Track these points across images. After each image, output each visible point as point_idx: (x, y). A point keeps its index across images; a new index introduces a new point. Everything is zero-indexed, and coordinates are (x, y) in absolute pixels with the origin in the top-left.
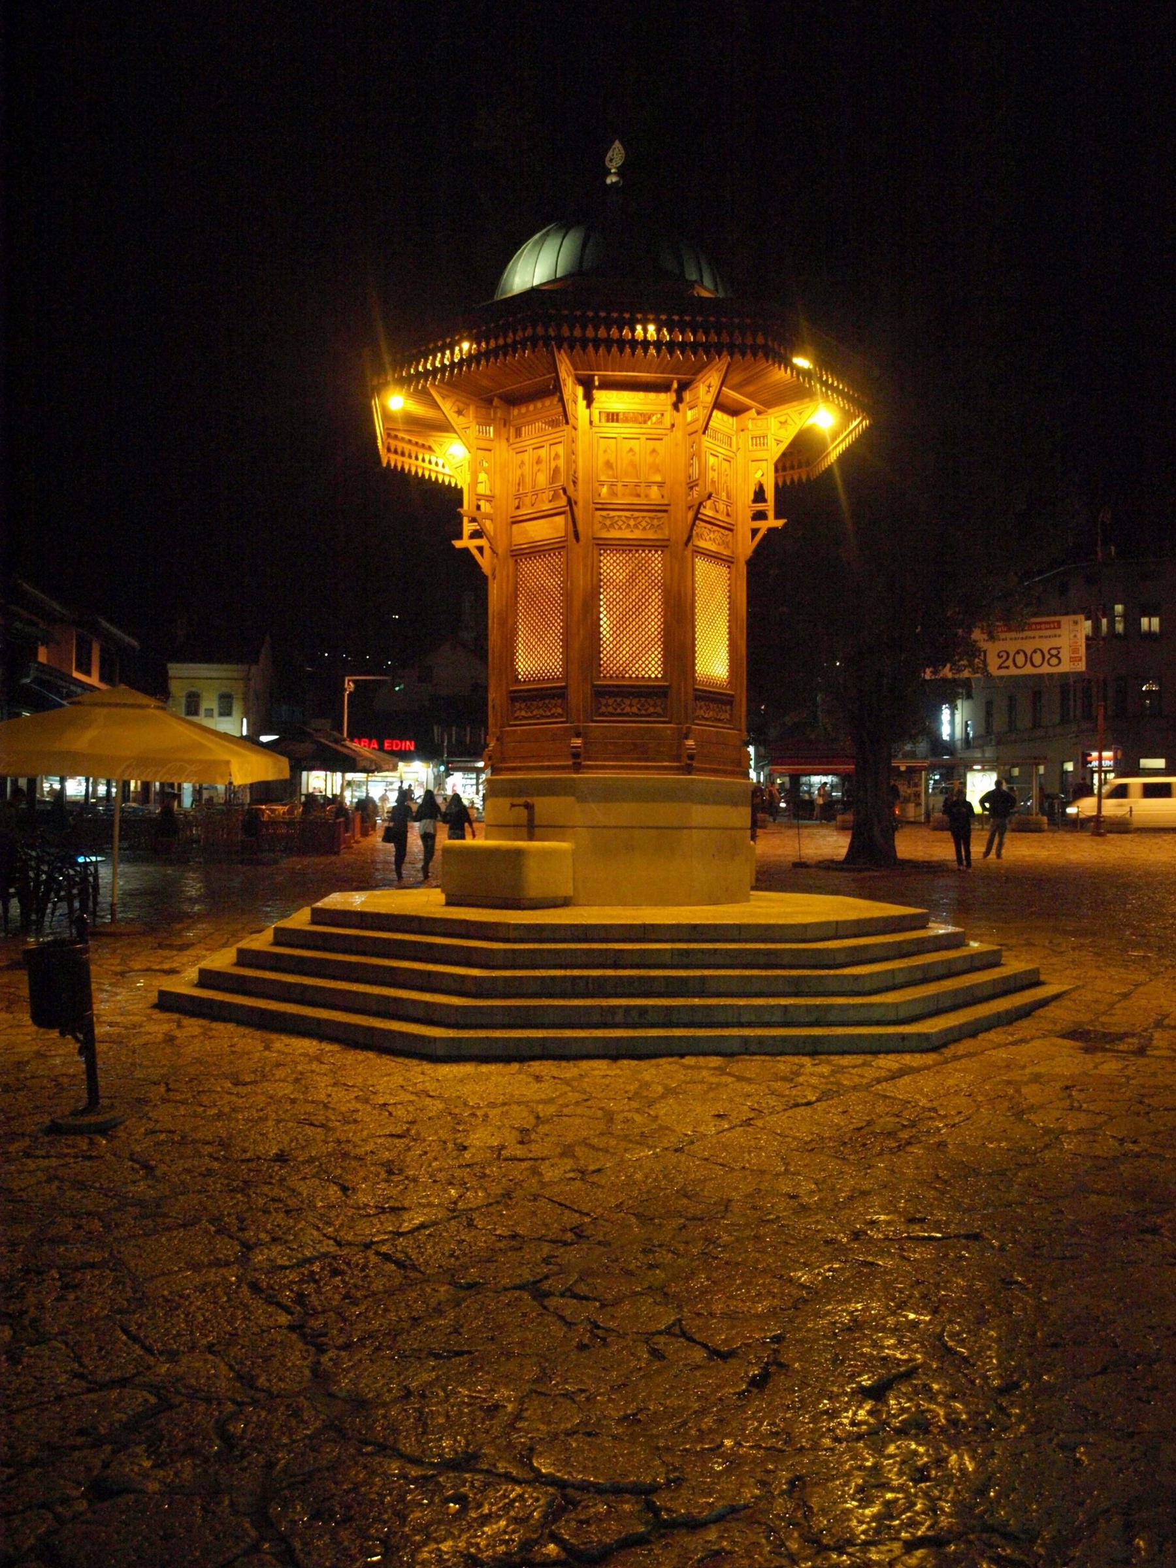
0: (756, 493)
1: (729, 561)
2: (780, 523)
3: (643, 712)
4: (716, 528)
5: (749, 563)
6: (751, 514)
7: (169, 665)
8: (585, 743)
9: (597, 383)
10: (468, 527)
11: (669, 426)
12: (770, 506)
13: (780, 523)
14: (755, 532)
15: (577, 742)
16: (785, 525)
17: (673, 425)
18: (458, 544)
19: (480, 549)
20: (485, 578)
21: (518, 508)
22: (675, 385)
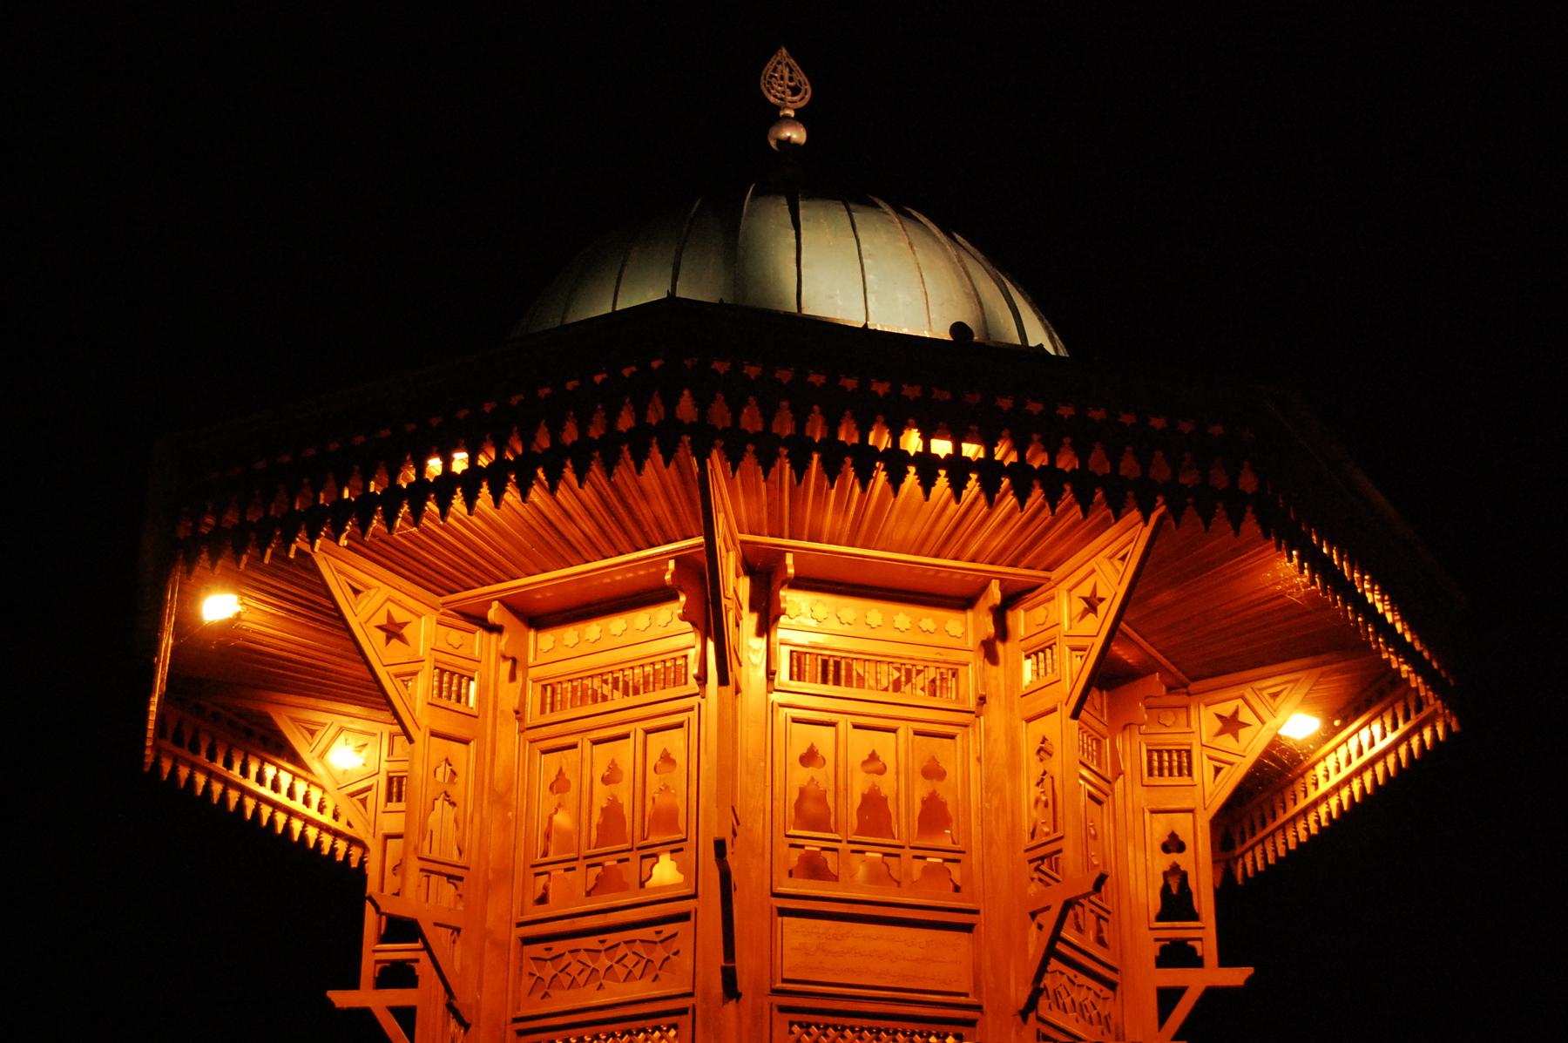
0: (1166, 890)
2: (1237, 976)
4: (1082, 979)
6: (1153, 950)
9: (791, 571)
10: (375, 953)
11: (972, 704)
12: (1204, 933)
13: (1237, 976)
14: (1168, 998)
16: (1249, 981)
17: (982, 700)
18: (341, 998)
19: (406, 1016)
21: (542, 900)
22: (995, 594)
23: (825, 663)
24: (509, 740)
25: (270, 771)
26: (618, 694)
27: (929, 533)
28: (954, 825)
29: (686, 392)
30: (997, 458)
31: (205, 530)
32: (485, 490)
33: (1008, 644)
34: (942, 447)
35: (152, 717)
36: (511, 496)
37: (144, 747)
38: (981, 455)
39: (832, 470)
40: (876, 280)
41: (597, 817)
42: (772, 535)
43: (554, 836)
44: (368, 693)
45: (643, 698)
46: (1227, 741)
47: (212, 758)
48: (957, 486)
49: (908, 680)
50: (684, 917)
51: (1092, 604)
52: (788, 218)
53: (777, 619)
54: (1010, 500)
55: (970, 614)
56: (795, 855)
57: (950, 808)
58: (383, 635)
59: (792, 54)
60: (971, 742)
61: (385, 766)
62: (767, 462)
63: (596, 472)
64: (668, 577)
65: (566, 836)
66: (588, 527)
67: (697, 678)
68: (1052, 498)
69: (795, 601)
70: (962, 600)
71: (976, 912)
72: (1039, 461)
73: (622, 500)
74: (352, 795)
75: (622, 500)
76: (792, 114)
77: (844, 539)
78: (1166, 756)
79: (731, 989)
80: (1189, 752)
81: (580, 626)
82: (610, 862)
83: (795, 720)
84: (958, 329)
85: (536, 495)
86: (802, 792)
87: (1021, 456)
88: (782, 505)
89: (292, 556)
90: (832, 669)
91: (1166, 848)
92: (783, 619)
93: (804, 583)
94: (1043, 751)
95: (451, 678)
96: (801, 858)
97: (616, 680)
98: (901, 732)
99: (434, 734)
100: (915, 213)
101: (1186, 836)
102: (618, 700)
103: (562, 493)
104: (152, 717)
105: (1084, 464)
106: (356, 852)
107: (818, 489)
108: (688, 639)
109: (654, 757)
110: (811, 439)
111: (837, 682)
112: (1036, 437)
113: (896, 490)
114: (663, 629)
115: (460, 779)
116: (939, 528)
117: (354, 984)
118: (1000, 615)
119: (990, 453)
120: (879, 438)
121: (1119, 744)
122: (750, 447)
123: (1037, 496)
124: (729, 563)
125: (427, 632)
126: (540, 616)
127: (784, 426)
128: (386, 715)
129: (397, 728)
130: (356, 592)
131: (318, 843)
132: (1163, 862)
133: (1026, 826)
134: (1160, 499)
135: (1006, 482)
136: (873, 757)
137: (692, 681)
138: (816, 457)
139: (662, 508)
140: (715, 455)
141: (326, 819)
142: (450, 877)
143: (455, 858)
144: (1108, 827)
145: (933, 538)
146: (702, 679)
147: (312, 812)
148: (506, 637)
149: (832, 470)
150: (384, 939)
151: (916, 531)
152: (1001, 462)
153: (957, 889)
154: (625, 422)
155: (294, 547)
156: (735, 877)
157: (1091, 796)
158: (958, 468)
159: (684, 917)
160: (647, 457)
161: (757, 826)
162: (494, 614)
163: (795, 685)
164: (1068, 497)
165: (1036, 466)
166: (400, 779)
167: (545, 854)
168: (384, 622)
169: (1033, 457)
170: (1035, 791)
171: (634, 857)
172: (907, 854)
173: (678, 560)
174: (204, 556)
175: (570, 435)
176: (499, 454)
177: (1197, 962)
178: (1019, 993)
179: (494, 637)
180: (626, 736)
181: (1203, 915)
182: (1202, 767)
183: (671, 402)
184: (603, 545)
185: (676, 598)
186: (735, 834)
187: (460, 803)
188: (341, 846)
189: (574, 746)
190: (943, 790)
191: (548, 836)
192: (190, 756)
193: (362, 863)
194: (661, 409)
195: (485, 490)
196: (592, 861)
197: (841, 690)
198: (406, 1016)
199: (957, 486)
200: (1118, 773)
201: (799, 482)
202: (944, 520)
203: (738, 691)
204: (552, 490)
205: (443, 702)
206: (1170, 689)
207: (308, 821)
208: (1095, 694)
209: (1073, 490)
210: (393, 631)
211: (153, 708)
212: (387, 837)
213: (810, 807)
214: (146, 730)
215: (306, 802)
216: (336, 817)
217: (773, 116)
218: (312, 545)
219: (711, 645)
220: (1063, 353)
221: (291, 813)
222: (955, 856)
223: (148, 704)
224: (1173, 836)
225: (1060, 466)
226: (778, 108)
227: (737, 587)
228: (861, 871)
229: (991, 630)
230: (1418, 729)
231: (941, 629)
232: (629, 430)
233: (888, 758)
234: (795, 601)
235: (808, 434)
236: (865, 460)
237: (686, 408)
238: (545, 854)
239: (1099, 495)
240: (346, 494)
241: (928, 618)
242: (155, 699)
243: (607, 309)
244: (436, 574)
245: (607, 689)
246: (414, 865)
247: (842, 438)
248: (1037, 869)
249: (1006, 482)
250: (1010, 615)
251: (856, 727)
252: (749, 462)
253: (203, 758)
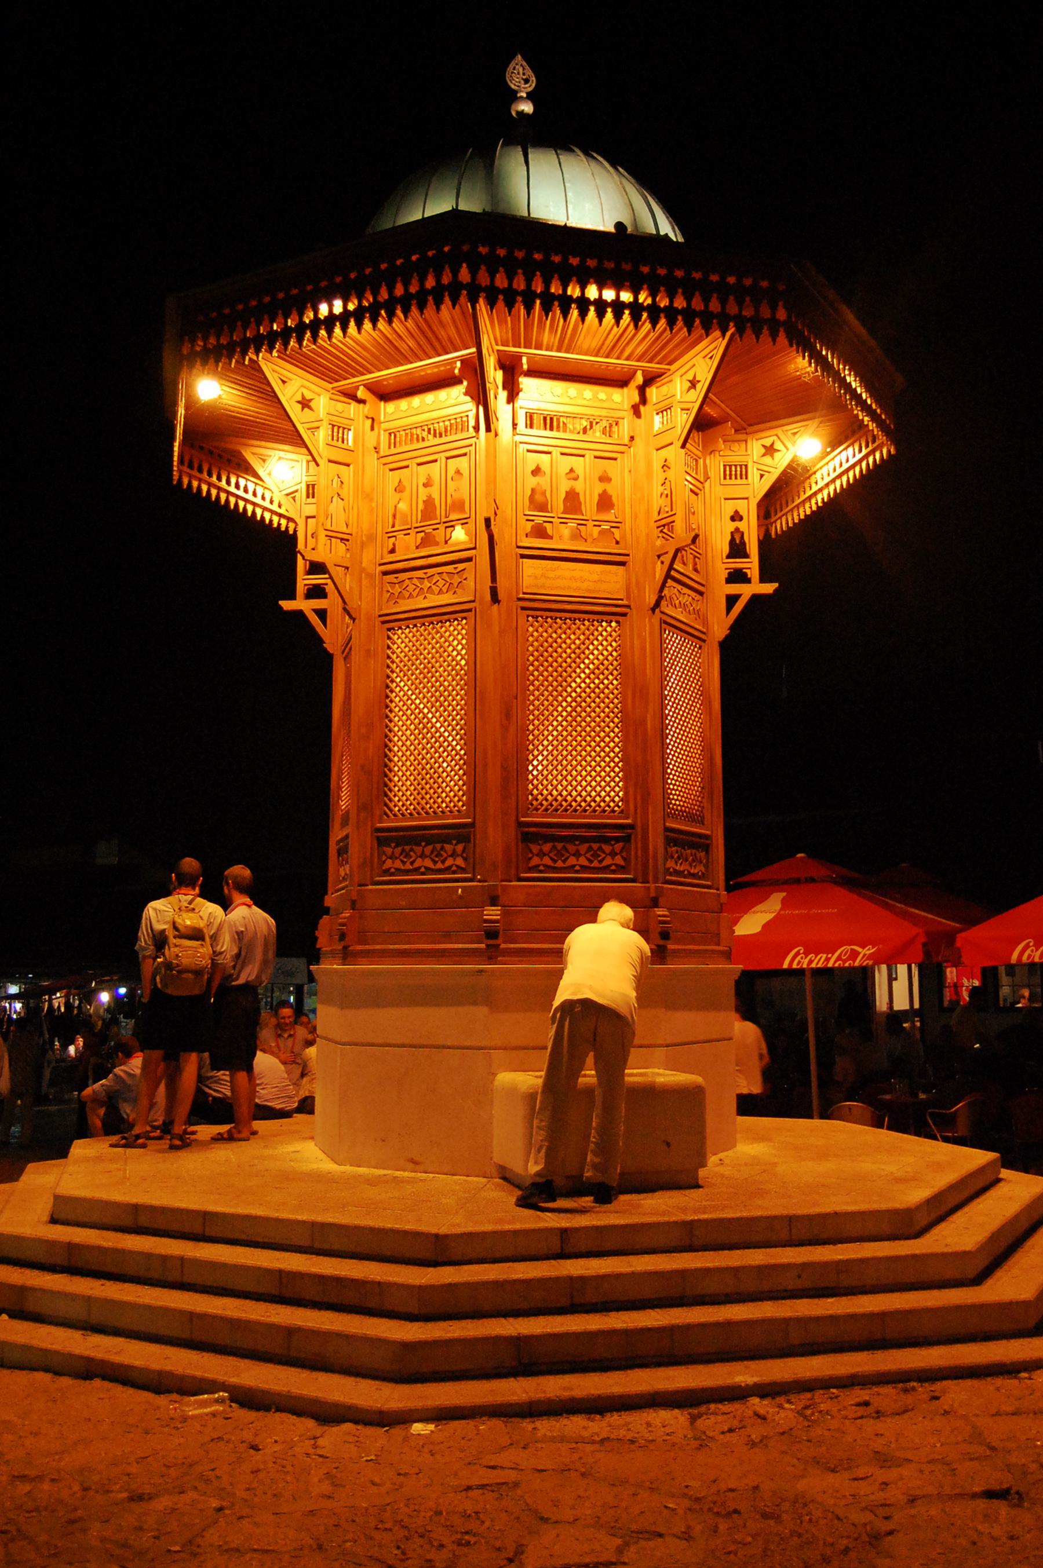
0: (732, 542)
1: (699, 638)
2: (769, 588)
3: (595, 864)
4: (685, 590)
5: (726, 646)
6: (724, 574)
8: (504, 914)
9: (525, 367)
10: (304, 580)
11: (626, 441)
12: (752, 565)
13: (769, 588)
14: (732, 600)
15: (493, 913)
16: (776, 591)
17: (632, 438)
18: (286, 605)
19: (322, 614)
20: (330, 656)
22: (639, 378)
23: (545, 419)
24: (372, 463)
25: (242, 482)
26: (430, 437)
27: (603, 344)
28: (616, 508)
29: (464, 265)
30: (641, 301)
31: (198, 349)
32: (352, 323)
33: (647, 406)
34: (609, 295)
35: (176, 454)
36: (367, 325)
37: (173, 470)
38: (631, 300)
39: (547, 309)
40: (573, 195)
41: (421, 506)
42: (514, 346)
43: (398, 516)
44: (294, 438)
45: (444, 439)
46: (767, 459)
47: (210, 475)
48: (618, 317)
49: (591, 427)
50: (469, 559)
51: (693, 384)
52: (523, 159)
53: (518, 394)
54: (648, 326)
55: (625, 390)
56: (530, 524)
57: (614, 499)
58: (300, 406)
59: (524, 58)
60: (625, 462)
61: (305, 479)
62: (510, 305)
63: (414, 311)
64: (457, 371)
65: (404, 515)
66: (411, 343)
67: (474, 428)
68: (671, 323)
69: (526, 383)
70: (621, 382)
71: (628, 555)
72: (664, 303)
73: (430, 327)
74: (287, 495)
75: (430, 327)
76: (525, 95)
77: (555, 348)
78: (733, 468)
79: (495, 598)
80: (746, 466)
81: (409, 399)
82: (429, 530)
83: (528, 451)
84: (619, 226)
85: (382, 324)
86: (533, 490)
87: (654, 300)
88: (519, 329)
89: (247, 363)
90: (550, 422)
91: (733, 519)
92: (521, 394)
93: (531, 373)
94: (665, 466)
95: (338, 429)
96: (532, 527)
97: (429, 429)
98: (587, 457)
99: (330, 461)
100: (595, 155)
101: (743, 513)
102: (432, 440)
103: (396, 324)
104: (176, 454)
105: (689, 303)
106: (292, 526)
107: (540, 320)
108: (468, 406)
109: (451, 472)
110: (535, 292)
111: (551, 429)
112: (662, 289)
113: (583, 321)
114: (454, 400)
115: (345, 486)
116: (608, 342)
117: (292, 597)
118: (642, 390)
119: (636, 299)
120: (573, 289)
121: (708, 461)
122: (501, 297)
123: (662, 323)
124: (490, 363)
125: (324, 403)
126: (386, 394)
127: (520, 284)
128: (304, 450)
129: (310, 458)
130: (284, 382)
131: (271, 521)
132: (732, 526)
133: (656, 509)
134: (732, 324)
135: (645, 315)
136: (572, 470)
137: (471, 430)
138: (538, 302)
139: (452, 331)
140: (481, 301)
141: (275, 507)
142: (342, 539)
143: (344, 529)
144: (701, 508)
145: (605, 347)
146: (477, 428)
147: (266, 504)
148: (368, 405)
149: (547, 309)
150: (309, 573)
151: (595, 344)
152: (642, 304)
153: (617, 543)
154: (430, 283)
155: (247, 358)
156: (496, 537)
157: (692, 490)
158: (618, 307)
159: (469, 559)
160: (442, 303)
161: (507, 510)
162: (361, 393)
163: (529, 431)
164: (680, 323)
165: (662, 305)
166: (313, 485)
167: (393, 526)
168: (300, 399)
169: (660, 301)
170: (661, 489)
171: (442, 527)
172: (590, 524)
173: (462, 361)
174: (198, 363)
175: (399, 291)
176: (360, 302)
177: (748, 581)
178: (651, 599)
179: (361, 406)
180: (436, 461)
181: (752, 555)
182: (753, 474)
183: (455, 272)
184: (420, 353)
185: (461, 382)
186: (496, 514)
187: (346, 500)
188: (283, 522)
189: (407, 467)
190: (612, 489)
191: (394, 516)
192: (198, 475)
193: (295, 531)
194: (450, 275)
195: (352, 323)
196: (419, 530)
197: (554, 434)
198: (322, 614)
199: (618, 317)
200: (707, 478)
201: (528, 314)
202: (611, 337)
203: (496, 435)
204: (390, 322)
205: (335, 443)
206: (736, 431)
207: (265, 509)
208: (695, 434)
209: (683, 319)
210: (305, 404)
211: (176, 449)
212: (308, 517)
213: (538, 497)
214: (173, 461)
215: (263, 498)
216: (280, 506)
217: (513, 96)
218: (258, 356)
219: (481, 409)
220: (681, 239)
221: (254, 504)
222: (617, 525)
223: (172, 446)
224: (736, 512)
225: (675, 305)
226: (516, 92)
227: (495, 376)
228: (565, 531)
229: (637, 399)
230: (873, 452)
231: (609, 398)
232: (433, 288)
233: (579, 471)
234: (526, 383)
235: (533, 288)
236: (566, 303)
237: (464, 275)
238: (393, 526)
239: (697, 321)
240: (275, 327)
241: (602, 393)
242: (177, 444)
243: (417, 216)
244: (326, 371)
245: (425, 434)
246: (322, 534)
247: (553, 290)
248: (661, 531)
249: (645, 315)
250: (648, 390)
251: (562, 454)
252: (501, 304)
253: (205, 475)
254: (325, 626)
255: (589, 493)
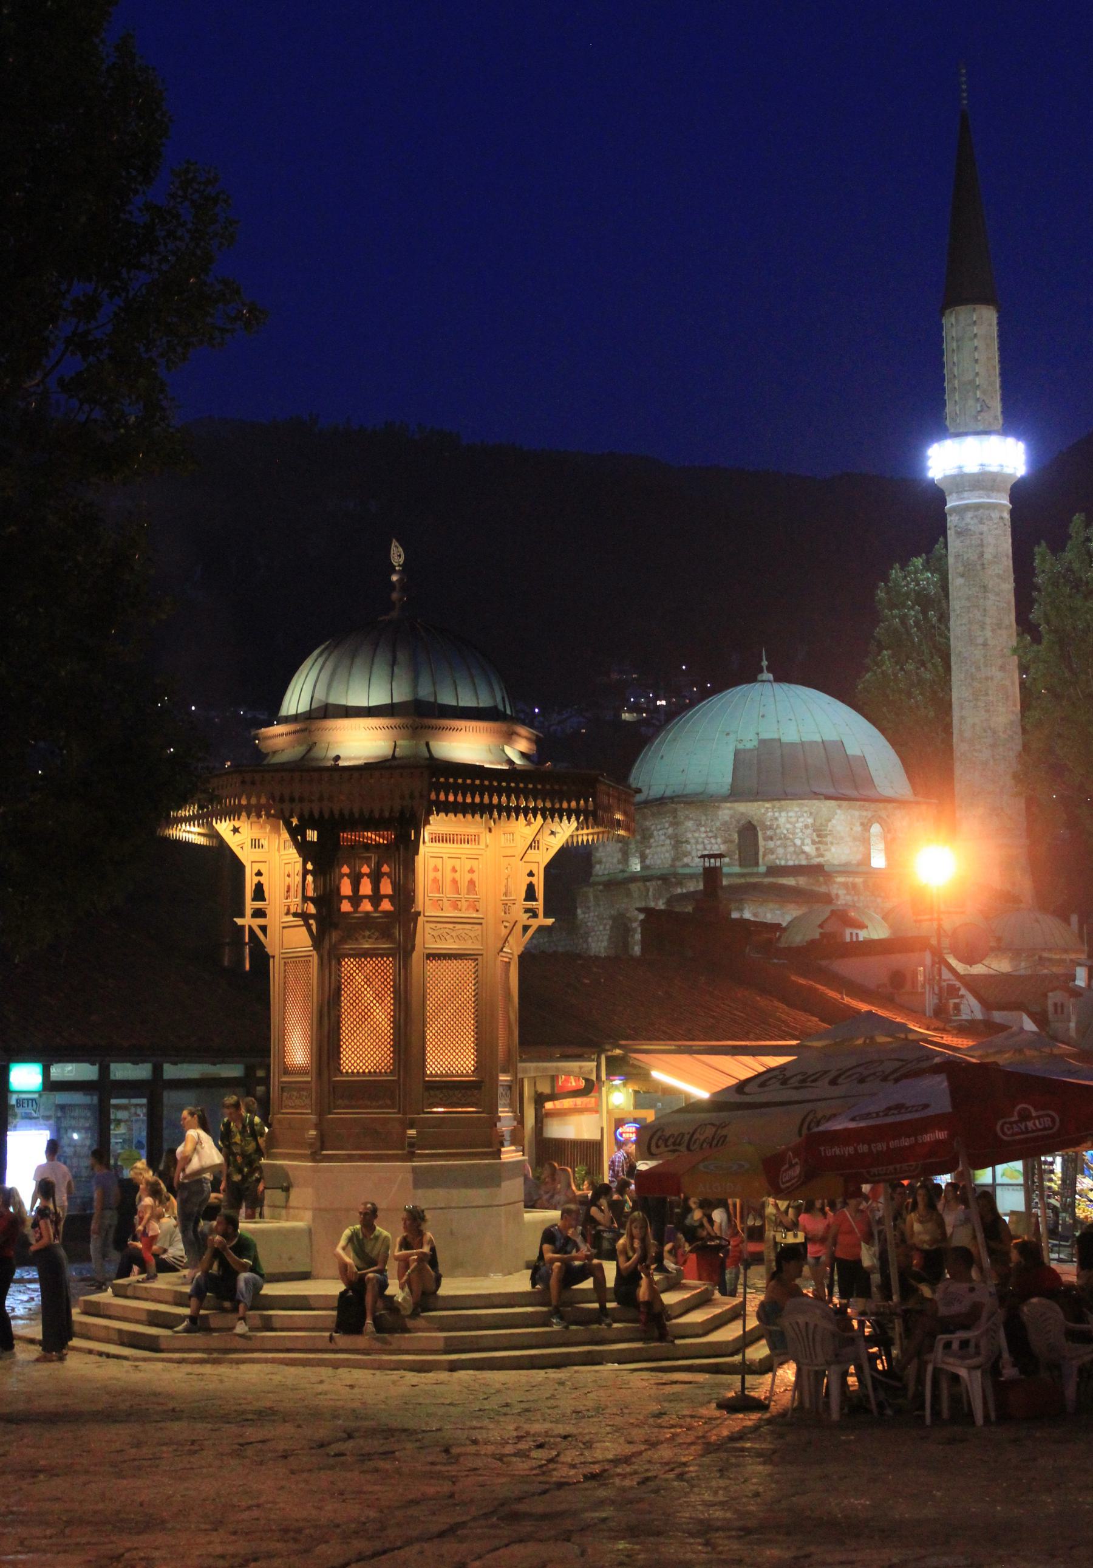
5: (520, 957)
7: (112, 1077)
12: (539, 905)
13: (550, 921)
14: (526, 928)
117: (242, 916)
150: (253, 900)
177: (535, 915)
198: (264, 929)
254: (266, 936)
255: (464, 878)
